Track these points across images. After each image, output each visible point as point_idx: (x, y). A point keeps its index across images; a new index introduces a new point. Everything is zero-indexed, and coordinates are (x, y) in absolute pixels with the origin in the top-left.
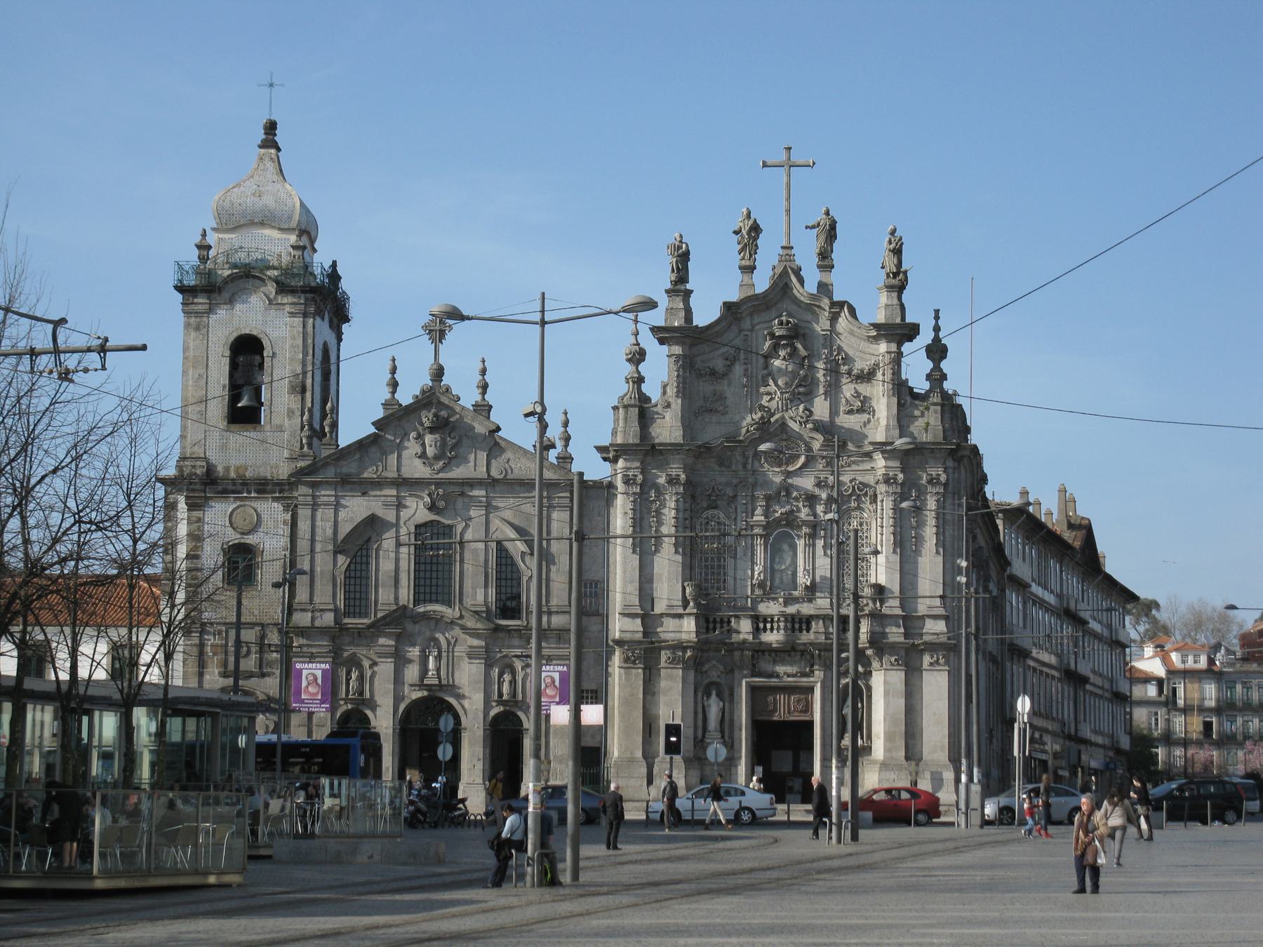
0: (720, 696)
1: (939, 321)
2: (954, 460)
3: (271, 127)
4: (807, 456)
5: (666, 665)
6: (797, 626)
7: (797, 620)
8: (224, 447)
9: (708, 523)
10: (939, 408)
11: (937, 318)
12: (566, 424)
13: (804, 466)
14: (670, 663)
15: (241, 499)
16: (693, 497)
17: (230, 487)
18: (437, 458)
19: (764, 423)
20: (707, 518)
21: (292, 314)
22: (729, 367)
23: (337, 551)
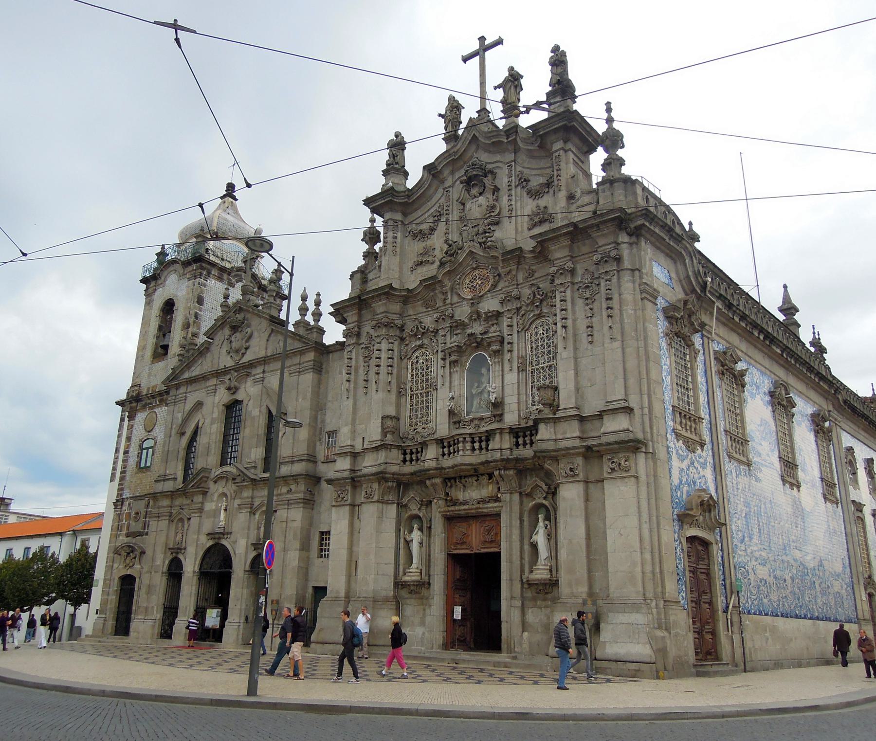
0: (421, 529)
1: (612, 114)
2: (630, 235)
5: (365, 500)
6: (477, 445)
7: (477, 439)
8: (149, 375)
9: (417, 362)
11: (609, 110)
12: (318, 303)
13: (494, 286)
14: (368, 498)
16: (402, 339)
17: (149, 401)
18: (237, 351)
19: (452, 255)
21: (189, 279)
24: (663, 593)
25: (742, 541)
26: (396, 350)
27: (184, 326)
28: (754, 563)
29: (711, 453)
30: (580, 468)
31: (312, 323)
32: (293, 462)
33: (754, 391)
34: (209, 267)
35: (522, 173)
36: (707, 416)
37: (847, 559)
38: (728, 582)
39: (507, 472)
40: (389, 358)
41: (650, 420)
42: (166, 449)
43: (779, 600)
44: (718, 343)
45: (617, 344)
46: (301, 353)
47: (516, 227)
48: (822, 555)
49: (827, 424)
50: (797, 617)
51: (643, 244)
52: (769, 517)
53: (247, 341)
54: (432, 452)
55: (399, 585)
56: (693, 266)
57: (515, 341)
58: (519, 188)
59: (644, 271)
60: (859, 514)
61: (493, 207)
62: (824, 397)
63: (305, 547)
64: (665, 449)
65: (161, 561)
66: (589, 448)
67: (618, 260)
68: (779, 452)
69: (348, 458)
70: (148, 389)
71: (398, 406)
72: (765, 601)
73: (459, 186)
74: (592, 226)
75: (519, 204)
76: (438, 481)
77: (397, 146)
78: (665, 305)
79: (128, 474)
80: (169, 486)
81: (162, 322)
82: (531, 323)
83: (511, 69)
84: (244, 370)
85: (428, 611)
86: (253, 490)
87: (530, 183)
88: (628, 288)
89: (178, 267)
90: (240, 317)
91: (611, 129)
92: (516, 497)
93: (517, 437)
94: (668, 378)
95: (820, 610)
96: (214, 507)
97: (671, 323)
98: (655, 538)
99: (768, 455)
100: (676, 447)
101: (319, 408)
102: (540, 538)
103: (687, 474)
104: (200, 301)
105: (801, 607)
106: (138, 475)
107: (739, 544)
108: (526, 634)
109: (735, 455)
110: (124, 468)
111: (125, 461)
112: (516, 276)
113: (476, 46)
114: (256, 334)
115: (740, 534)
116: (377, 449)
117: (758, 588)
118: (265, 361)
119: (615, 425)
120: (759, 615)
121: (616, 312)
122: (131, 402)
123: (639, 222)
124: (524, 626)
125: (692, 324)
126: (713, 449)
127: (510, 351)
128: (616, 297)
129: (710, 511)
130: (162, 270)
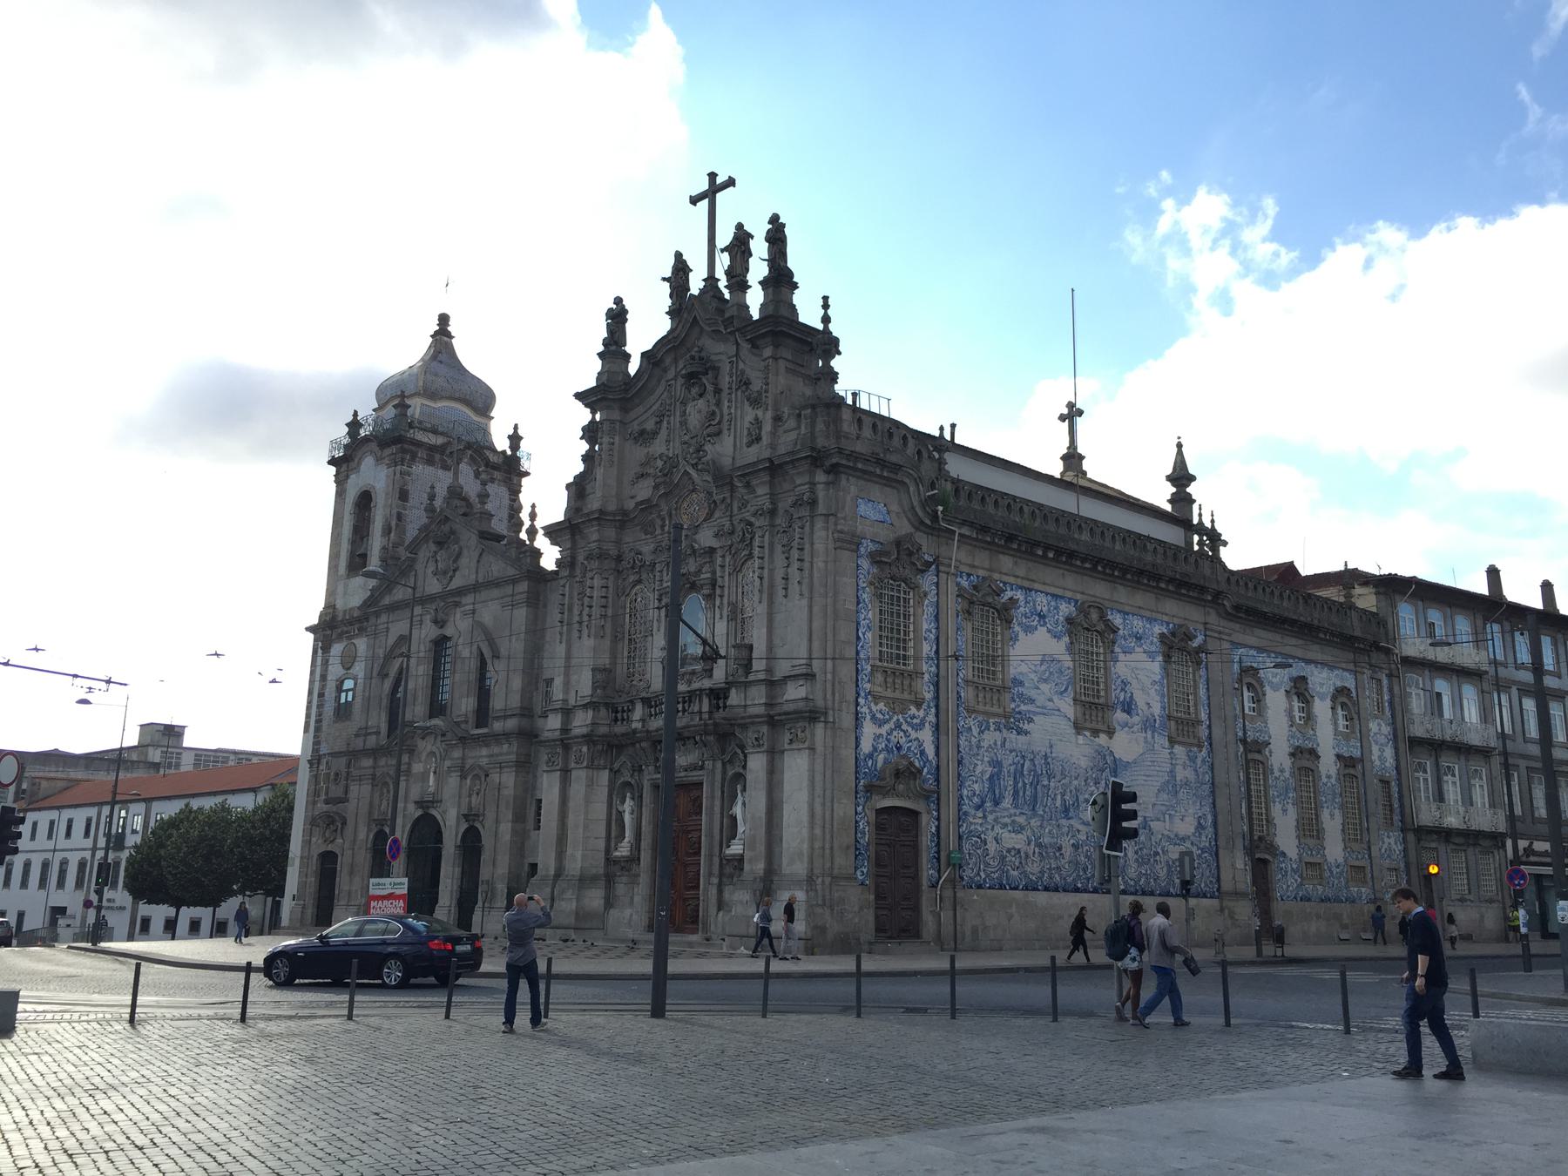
0: (633, 799)
1: (829, 312)
2: (828, 472)
3: (444, 319)
4: (709, 504)
6: (680, 707)
7: (680, 700)
8: (345, 593)
10: (809, 411)
11: (826, 306)
15: (349, 638)
17: (345, 629)
18: (445, 573)
20: (636, 594)
21: (389, 466)
22: (659, 423)
23: (383, 675)
24: (832, 868)
25: (978, 807)
26: (611, 585)
27: (383, 529)
28: (998, 829)
29: (933, 710)
30: (765, 738)
31: (528, 543)
32: (505, 717)
33: (1035, 623)
34: (413, 448)
35: (743, 372)
36: (933, 669)
37: (1210, 818)
38: (942, 853)
39: (708, 738)
40: (602, 597)
41: (833, 685)
42: (367, 694)
43: (1042, 872)
44: (969, 575)
45: (805, 602)
46: (514, 581)
47: (735, 442)
48: (1147, 815)
49: (1195, 644)
50: (1077, 890)
51: (844, 482)
52: (1037, 777)
53: (455, 561)
54: (639, 712)
55: (609, 860)
56: (919, 494)
57: (727, 585)
58: (739, 393)
59: (839, 515)
60: (1257, 756)
61: (713, 413)
62: (1199, 605)
63: (519, 818)
64: (853, 716)
65: (364, 834)
66: (771, 717)
67: (813, 503)
68: (1075, 692)
69: (559, 716)
70: (345, 615)
71: (614, 656)
72: (1016, 873)
73: (680, 381)
74: (787, 463)
75: (739, 412)
76: (644, 744)
77: (617, 317)
78: (872, 547)
79: (325, 723)
80: (372, 741)
81: (357, 522)
82: (743, 564)
83: (740, 226)
84: (452, 598)
85: (636, 890)
86: (464, 749)
87: (751, 387)
88: (820, 533)
89: (373, 446)
90: (446, 528)
91: (827, 331)
92: (719, 765)
93: (718, 698)
94: (869, 635)
95: (1132, 883)
96: (422, 770)
97: (882, 570)
98: (828, 814)
99: (1051, 700)
100: (871, 711)
101: (535, 651)
102: (738, 810)
103: (888, 740)
104: (404, 495)
105: (1088, 879)
106: (337, 725)
107: (972, 812)
108: (721, 914)
109: (981, 707)
110: (320, 715)
111: (320, 706)
112: (731, 505)
113: (704, 185)
114: (465, 552)
115: (976, 799)
116: (585, 706)
117: (1003, 858)
118: (475, 588)
119: (795, 692)
120: (1001, 889)
121: (806, 565)
122: (324, 630)
123: (834, 461)
124: (721, 906)
125: (914, 564)
126: (937, 707)
127: (721, 596)
128: (807, 546)
129: (915, 779)
130: (354, 450)
